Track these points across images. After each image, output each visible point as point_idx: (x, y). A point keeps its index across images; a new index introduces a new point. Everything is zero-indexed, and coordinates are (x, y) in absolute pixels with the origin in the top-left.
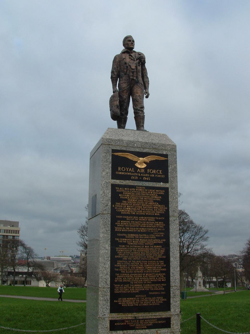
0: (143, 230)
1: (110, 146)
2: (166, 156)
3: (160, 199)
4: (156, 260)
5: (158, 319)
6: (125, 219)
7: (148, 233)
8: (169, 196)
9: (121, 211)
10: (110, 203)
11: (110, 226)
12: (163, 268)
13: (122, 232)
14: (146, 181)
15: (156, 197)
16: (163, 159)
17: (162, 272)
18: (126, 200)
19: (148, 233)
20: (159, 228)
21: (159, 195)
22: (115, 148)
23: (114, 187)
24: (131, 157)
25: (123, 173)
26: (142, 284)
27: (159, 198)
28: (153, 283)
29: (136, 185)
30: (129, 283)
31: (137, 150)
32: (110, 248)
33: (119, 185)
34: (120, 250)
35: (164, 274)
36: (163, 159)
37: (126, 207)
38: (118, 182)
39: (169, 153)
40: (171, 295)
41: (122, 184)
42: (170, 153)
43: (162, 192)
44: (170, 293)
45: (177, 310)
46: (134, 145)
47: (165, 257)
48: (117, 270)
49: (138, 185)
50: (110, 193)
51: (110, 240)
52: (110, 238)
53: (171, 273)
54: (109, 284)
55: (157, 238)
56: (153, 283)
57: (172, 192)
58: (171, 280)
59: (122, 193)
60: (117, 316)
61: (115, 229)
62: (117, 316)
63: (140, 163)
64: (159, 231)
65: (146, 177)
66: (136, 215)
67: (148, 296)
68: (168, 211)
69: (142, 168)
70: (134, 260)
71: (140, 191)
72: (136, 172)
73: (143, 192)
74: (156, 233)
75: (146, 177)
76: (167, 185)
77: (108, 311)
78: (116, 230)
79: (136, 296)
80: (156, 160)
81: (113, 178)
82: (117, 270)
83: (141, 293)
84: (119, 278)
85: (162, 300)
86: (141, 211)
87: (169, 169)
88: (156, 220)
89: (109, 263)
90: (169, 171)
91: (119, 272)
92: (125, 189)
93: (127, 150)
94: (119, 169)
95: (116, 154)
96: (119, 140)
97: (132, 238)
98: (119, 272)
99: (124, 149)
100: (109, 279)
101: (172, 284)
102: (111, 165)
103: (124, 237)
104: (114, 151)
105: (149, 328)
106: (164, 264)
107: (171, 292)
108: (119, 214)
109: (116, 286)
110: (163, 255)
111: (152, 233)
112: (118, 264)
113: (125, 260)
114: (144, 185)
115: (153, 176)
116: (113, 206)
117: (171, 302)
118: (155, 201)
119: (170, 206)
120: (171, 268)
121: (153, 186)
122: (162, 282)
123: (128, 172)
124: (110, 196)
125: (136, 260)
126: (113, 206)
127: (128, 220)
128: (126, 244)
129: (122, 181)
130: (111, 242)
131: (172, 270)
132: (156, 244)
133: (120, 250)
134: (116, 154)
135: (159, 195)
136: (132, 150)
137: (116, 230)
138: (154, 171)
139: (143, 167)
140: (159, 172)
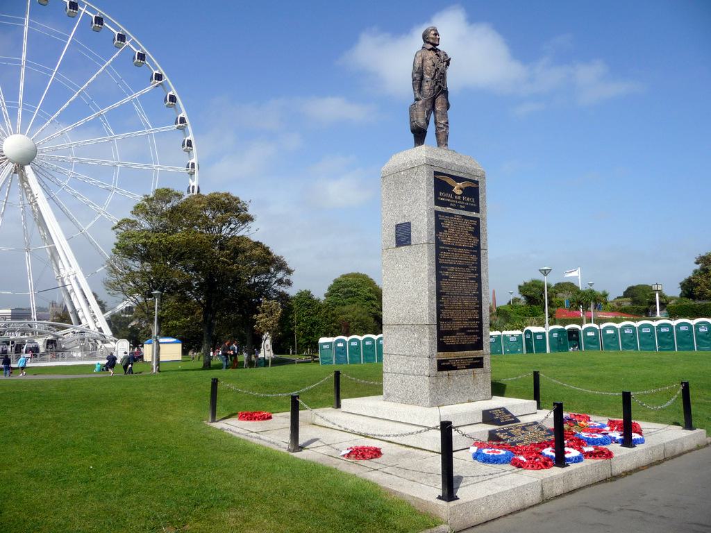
0: (460, 263)
2: (477, 183)
5: (475, 359)
6: (446, 251)
7: (465, 266)
10: (434, 233)
12: (477, 304)
13: (444, 265)
14: (463, 209)
17: (476, 308)
18: (447, 229)
19: (465, 266)
21: (472, 226)
22: (439, 170)
23: (437, 213)
24: (450, 181)
28: (470, 320)
31: (455, 174)
34: (444, 284)
36: (475, 185)
39: (479, 180)
40: (484, 333)
43: (475, 223)
55: (472, 272)
59: (443, 221)
60: (444, 356)
62: (444, 355)
64: (474, 265)
65: (462, 205)
67: (469, 334)
68: (479, 242)
72: (454, 199)
75: (462, 205)
76: (478, 215)
77: (436, 350)
83: (462, 330)
84: (443, 316)
85: (475, 338)
88: (472, 253)
89: (435, 298)
94: (441, 193)
95: (438, 177)
96: (439, 161)
98: (443, 308)
101: (484, 322)
102: (433, 189)
103: (446, 270)
104: (436, 173)
105: (468, 367)
108: (442, 244)
111: (468, 267)
118: (469, 232)
122: (476, 320)
124: (434, 224)
125: (456, 295)
128: (448, 277)
132: (471, 279)
133: (444, 284)
134: (438, 177)
135: (472, 226)
136: (450, 173)
138: (468, 199)
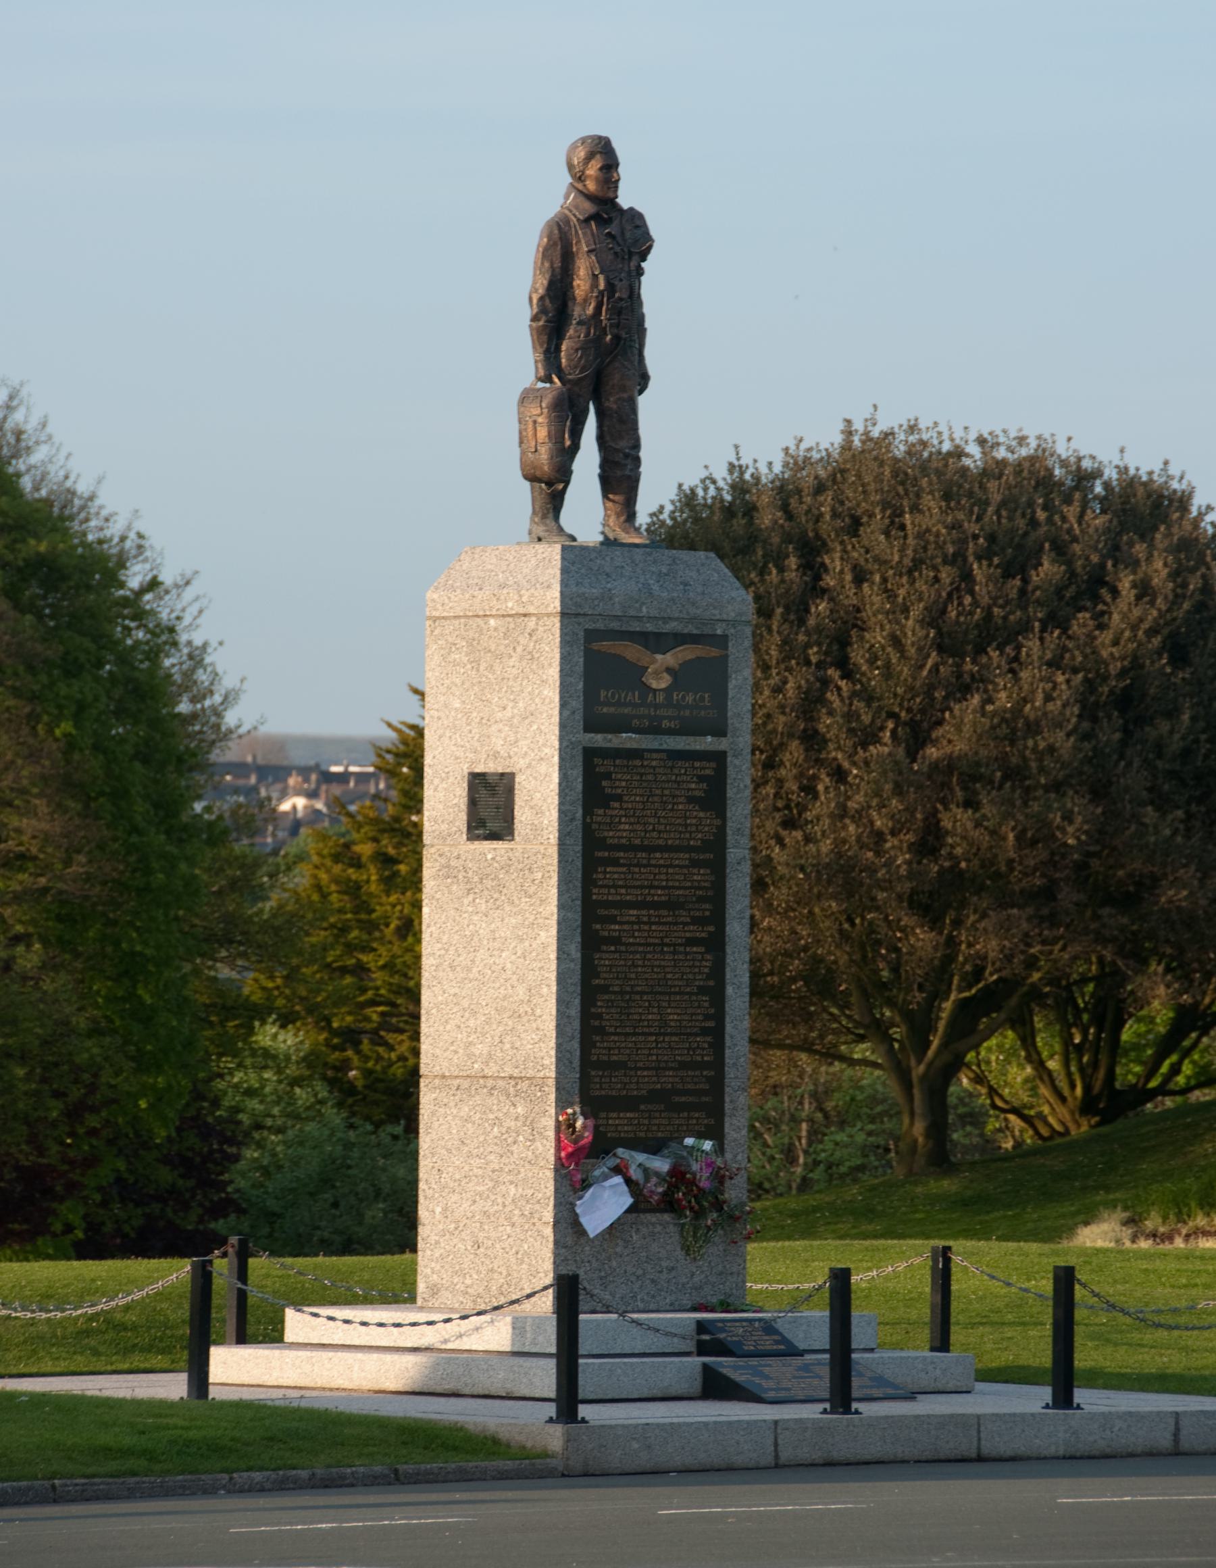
0: (659, 895)
1: (581, 620)
3: (705, 791)
4: (690, 994)
6: (615, 862)
7: (672, 905)
8: (729, 781)
9: (606, 834)
11: (580, 885)
15: (693, 786)
16: (715, 652)
17: (705, 1031)
18: (619, 798)
19: (672, 905)
20: (699, 888)
21: (701, 779)
24: (632, 652)
25: (612, 710)
26: (656, 1069)
27: (697, 788)
28: (683, 1066)
29: (644, 746)
30: (621, 1065)
31: (650, 627)
32: (579, 955)
33: (601, 748)
35: (709, 1039)
36: (715, 652)
37: (620, 823)
38: (599, 740)
41: (609, 745)
42: (732, 631)
44: (723, 1102)
45: (739, 1157)
46: (641, 610)
47: (711, 983)
48: (597, 1023)
49: (650, 746)
50: (580, 779)
51: (579, 930)
52: (579, 923)
53: (727, 1037)
54: (578, 1069)
55: (695, 921)
56: (683, 1066)
57: (735, 766)
58: (727, 1061)
59: (608, 776)
61: (592, 894)
63: (656, 673)
66: (642, 848)
69: (660, 690)
70: (637, 993)
71: (654, 768)
73: (661, 770)
74: (691, 906)
75: (670, 719)
76: (722, 744)
78: (594, 897)
79: (642, 1107)
80: (698, 658)
81: (588, 728)
82: (597, 1023)
86: (655, 834)
87: (731, 686)
88: (695, 864)
89: (577, 1001)
90: (731, 694)
91: (601, 1031)
92: (618, 762)
93: (624, 629)
94: (603, 693)
95: (595, 646)
97: (632, 923)
98: (601, 1031)
99: (615, 625)
100: (578, 1053)
103: (612, 920)
106: (711, 1006)
107: (727, 1099)
109: (593, 1073)
110: (709, 977)
112: (599, 1004)
113: (615, 993)
114: (665, 747)
115: (687, 713)
116: (588, 820)
117: (726, 1130)
118: (691, 800)
119: (729, 814)
120: (728, 1019)
121: (687, 748)
122: (702, 1066)
123: (625, 705)
124: (580, 787)
126: (588, 820)
127: (623, 865)
128: (616, 941)
129: (610, 736)
130: (583, 934)
131: (729, 1028)
134: (595, 646)
135: (701, 779)
136: (636, 627)
137: (594, 897)
138: (690, 699)
139: (663, 686)
140: (702, 699)
